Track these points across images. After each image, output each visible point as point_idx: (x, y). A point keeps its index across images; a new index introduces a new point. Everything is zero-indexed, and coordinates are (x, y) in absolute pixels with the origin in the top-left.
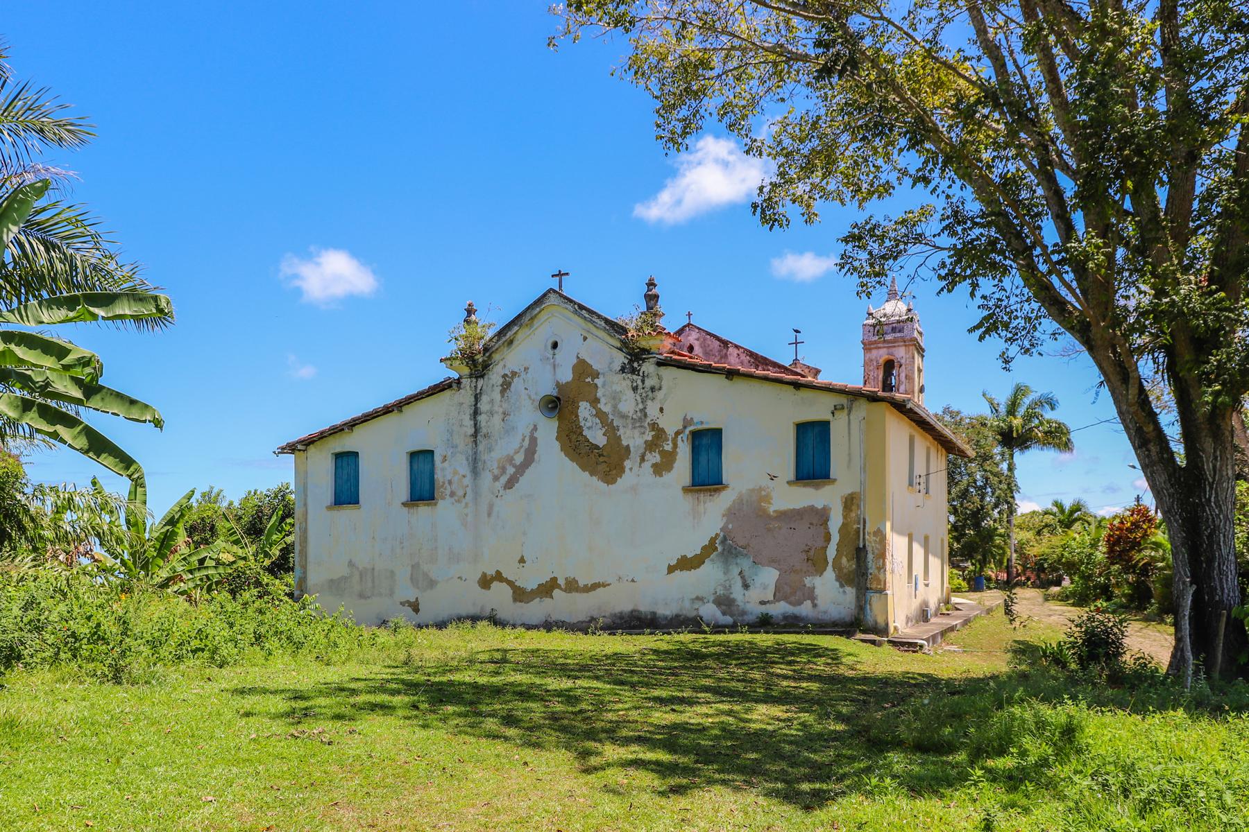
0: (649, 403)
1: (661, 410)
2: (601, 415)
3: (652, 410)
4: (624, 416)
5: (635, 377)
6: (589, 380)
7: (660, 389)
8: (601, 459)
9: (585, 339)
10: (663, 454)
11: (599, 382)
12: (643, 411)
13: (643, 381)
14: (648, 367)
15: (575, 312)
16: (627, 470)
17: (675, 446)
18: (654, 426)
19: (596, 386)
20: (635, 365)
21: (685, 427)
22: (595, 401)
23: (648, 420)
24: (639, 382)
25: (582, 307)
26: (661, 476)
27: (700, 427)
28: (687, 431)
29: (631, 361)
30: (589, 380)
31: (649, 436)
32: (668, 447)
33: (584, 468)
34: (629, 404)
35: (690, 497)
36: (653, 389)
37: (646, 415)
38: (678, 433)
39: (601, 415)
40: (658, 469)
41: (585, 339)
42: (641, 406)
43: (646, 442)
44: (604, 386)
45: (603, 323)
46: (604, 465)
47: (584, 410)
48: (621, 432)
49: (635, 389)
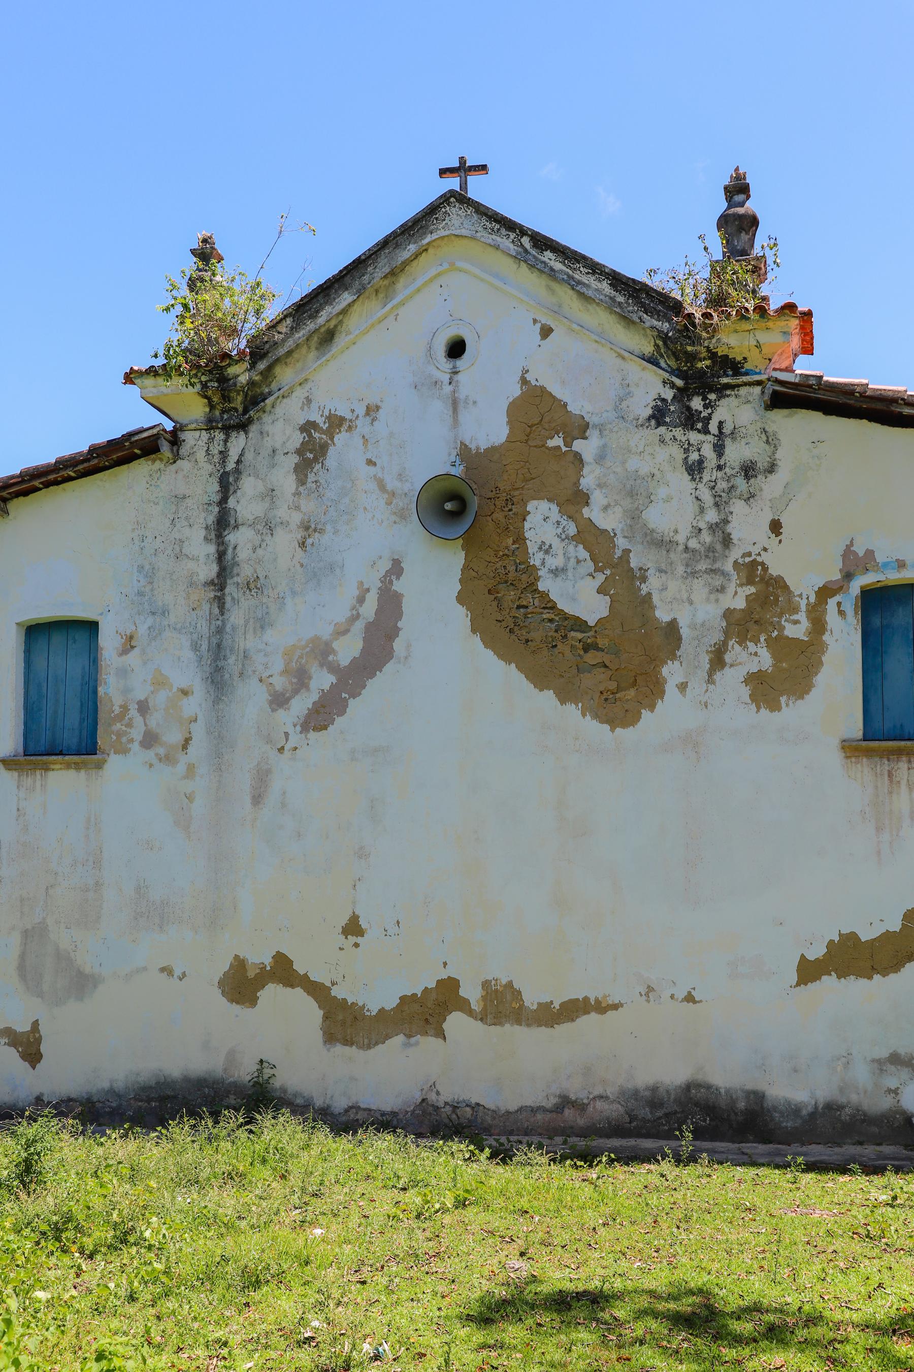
0: (738, 507)
1: (776, 527)
2: (592, 538)
3: (748, 527)
4: (663, 544)
5: (694, 437)
6: (557, 441)
7: (771, 468)
8: (592, 658)
9: (546, 332)
10: (781, 646)
11: (586, 448)
13: (719, 449)
14: (737, 410)
15: (522, 257)
16: (671, 689)
17: (818, 626)
18: (752, 570)
19: (578, 459)
20: (696, 403)
21: (848, 576)
22: (574, 500)
23: (735, 554)
24: (708, 451)
25: (542, 243)
26: (775, 707)
27: (893, 577)
28: (855, 586)
29: (683, 394)
30: (557, 441)
31: (738, 598)
32: (797, 629)
33: (540, 680)
34: (676, 508)
35: (865, 773)
36: (748, 470)
37: (727, 541)
38: (825, 592)
39: (592, 538)
40: (765, 690)
41: (546, 332)
42: (712, 516)
43: (728, 614)
44: (600, 458)
45: (605, 286)
46: (601, 675)
47: (542, 523)
48: (653, 584)
49: (695, 469)
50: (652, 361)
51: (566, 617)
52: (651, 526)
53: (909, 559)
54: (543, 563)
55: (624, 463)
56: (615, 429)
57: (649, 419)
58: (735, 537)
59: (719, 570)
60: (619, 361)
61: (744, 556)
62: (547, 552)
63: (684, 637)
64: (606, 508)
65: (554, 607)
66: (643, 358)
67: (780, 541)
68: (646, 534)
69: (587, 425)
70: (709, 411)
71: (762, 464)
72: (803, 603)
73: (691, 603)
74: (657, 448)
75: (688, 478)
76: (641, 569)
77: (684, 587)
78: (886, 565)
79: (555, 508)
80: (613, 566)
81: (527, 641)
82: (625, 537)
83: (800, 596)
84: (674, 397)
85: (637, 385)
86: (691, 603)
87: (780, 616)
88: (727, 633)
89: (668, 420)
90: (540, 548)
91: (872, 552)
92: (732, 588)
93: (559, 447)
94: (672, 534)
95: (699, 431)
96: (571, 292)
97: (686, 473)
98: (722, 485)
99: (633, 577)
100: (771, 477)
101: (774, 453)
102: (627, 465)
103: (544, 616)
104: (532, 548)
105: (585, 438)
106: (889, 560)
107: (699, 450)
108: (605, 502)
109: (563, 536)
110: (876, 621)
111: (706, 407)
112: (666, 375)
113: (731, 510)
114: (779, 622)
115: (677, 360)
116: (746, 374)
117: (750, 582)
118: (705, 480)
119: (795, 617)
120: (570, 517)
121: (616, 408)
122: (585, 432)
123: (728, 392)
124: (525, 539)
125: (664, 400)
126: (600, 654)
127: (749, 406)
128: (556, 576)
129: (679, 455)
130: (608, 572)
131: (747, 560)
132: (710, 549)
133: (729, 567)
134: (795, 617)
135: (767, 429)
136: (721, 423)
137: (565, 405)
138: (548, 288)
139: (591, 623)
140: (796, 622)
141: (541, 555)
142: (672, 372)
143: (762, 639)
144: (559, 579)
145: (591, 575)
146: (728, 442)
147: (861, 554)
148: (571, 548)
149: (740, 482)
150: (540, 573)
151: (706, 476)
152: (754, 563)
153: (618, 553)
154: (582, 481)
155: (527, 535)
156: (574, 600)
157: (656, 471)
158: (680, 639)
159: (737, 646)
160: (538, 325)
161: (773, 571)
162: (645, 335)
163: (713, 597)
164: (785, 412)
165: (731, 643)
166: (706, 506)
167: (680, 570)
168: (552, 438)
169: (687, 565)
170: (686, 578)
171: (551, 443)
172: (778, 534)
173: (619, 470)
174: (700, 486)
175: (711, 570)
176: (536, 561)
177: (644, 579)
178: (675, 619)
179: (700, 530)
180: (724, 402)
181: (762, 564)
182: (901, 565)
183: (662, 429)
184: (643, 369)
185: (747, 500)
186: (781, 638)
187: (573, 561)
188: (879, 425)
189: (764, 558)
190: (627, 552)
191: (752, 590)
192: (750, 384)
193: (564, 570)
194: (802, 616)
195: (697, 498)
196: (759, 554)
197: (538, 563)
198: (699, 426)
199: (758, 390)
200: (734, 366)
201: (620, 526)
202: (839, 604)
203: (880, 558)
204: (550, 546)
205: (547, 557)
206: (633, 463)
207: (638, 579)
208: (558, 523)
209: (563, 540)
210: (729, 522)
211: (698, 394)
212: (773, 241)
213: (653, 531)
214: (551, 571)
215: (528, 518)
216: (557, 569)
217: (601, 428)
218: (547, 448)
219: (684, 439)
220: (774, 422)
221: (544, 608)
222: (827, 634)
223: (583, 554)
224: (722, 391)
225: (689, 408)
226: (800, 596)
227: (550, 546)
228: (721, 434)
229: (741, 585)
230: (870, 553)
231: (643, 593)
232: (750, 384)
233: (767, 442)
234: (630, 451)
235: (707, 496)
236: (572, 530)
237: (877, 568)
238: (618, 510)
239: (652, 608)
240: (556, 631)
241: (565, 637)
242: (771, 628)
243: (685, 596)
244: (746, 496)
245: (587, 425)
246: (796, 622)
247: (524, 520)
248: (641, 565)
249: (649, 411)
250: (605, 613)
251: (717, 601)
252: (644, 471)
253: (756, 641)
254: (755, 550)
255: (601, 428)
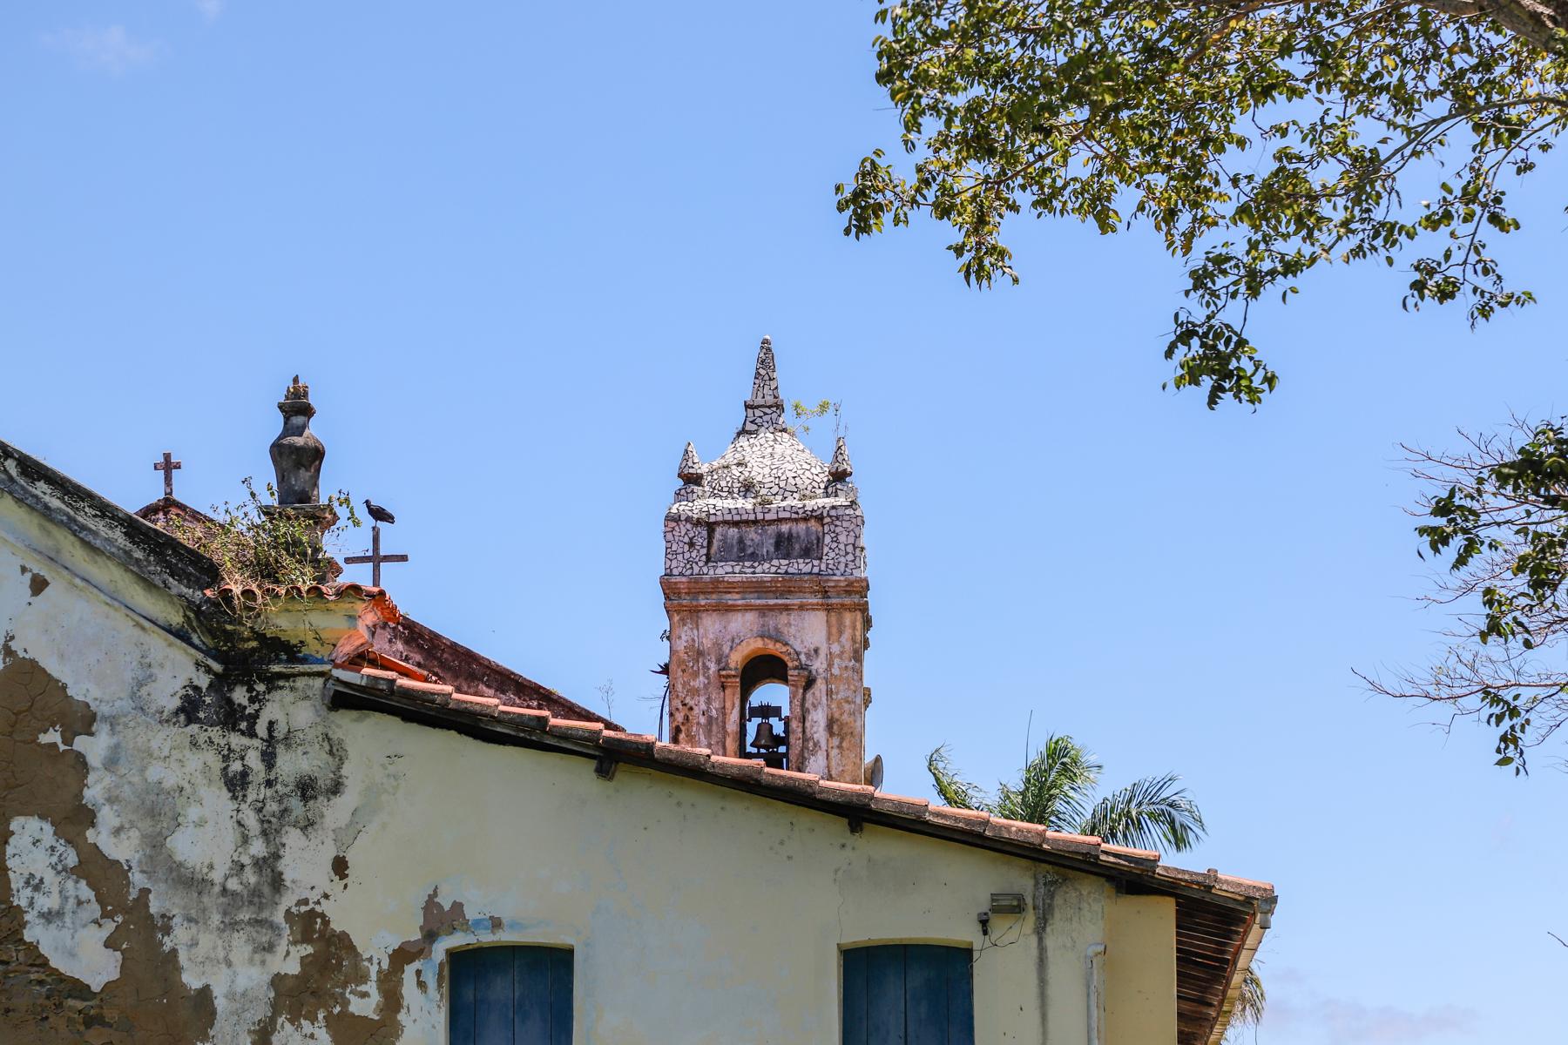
0: (292, 838)
1: (340, 866)
2: (98, 872)
3: (305, 866)
4: (190, 882)
5: (236, 740)
6: (52, 737)
7: (336, 788)
9: (39, 585)
11: (93, 747)
12: (269, 866)
13: (269, 759)
14: (291, 708)
17: (392, 1001)
18: (309, 924)
19: (81, 764)
20: (240, 695)
21: (430, 936)
22: (75, 819)
23: (288, 901)
24: (254, 760)
27: (487, 938)
28: (440, 950)
29: (221, 683)
30: (52, 737)
31: (290, 960)
32: (365, 1004)
34: (210, 836)
36: (306, 788)
37: (277, 883)
38: (402, 956)
39: (98, 872)
41: (39, 585)
42: (258, 848)
43: (277, 981)
44: (111, 763)
48: (180, 936)
49: (236, 784)
50: (181, 635)
51: (61, 978)
52: (178, 858)
53: (505, 915)
54: (31, 904)
55: (143, 770)
56: (132, 724)
57: (177, 713)
58: (288, 877)
59: (266, 921)
60: (137, 631)
61: (299, 903)
62: (37, 888)
63: (219, 1010)
64: (117, 831)
65: (44, 963)
66: (168, 630)
67: (346, 886)
68: (171, 870)
69: (92, 718)
70: (256, 706)
71: (324, 781)
72: (374, 970)
73: (229, 964)
74: (187, 752)
75: (226, 794)
76: (163, 916)
77: (220, 942)
78: (478, 923)
79: (48, 828)
80: (126, 911)
81: (7, 1011)
82: (142, 872)
83: (370, 960)
84: (211, 685)
85: (162, 666)
86: (229, 964)
87: (344, 987)
88: (276, 1008)
89: (202, 715)
90: (27, 883)
91: (461, 905)
92: (282, 948)
93: (54, 745)
94: (205, 870)
95: (243, 733)
96: (72, 538)
97: (225, 790)
98: (272, 807)
99: (154, 927)
100: (336, 800)
101: (339, 768)
102: (148, 773)
103: (32, 977)
104: (16, 882)
105: (92, 734)
106: (481, 916)
107: (242, 758)
108: (116, 822)
109: (60, 868)
110: (469, 994)
111: (252, 700)
112: (200, 656)
113: (284, 840)
114: (343, 994)
115: (214, 638)
116: (304, 661)
117: (306, 939)
118: (249, 800)
119: (363, 988)
120: (68, 842)
121: (133, 696)
122: (91, 725)
123: (281, 683)
124: (7, 869)
125: (196, 689)
126: (107, 1030)
127: (307, 703)
128: (49, 922)
129: (216, 764)
130: (120, 919)
131: (303, 909)
132: (255, 893)
133: (279, 918)
134: (363, 988)
135: (330, 735)
136: (271, 723)
137: (64, 687)
138: (42, 528)
139: (96, 988)
140: (365, 995)
141: (28, 892)
142: (207, 653)
143: (320, 1016)
144: (53, 926)
145: (96, 922)
146: (280, 749)
147: (447, 908)
148: (70, 884)
149: (295, 803)
150: (27, 917)
151: (251, 796)
152: (312, 914)
153: (134, 894)
154: (87, 793)
155: (9, 864)
156: (72, 955)
157: (186, 785)
158: (213, 1013)
159: (287, 1025)
160: (28, 576)
161: (336, 926)
162: (172, 603)
163: (257, 957)
164: (354, 714)
165: (280, 1021)
166: (251, 834)
167: (216, 919)
168: (45, 731)
169: (225, 914)
170: (223, 931)
171: (44, 739)
172: (343, 876)
173: (136, 779)
174: (243, 806)
175: (257, 921)
176: (21, 900)
177: (167, 930)
178: (208, 986)
179: (243, 866)
180: (276, 695)
181: (323, 916)
182: (496, 924)
183: (194, 728)
184: (170, 645)
185: (304, 829)
186: (346, 1015)
187: (72, 902)
188: (470, 740)
189: (325, 907)
190: (145, 892)
191: (309, 949)
192: (309, 675)
193: (60, 914)
194: (371, 987)
195: (239, 823)
196: (318, 903)
197: (23, 903)
198: (243, 725)
199: (319, 682)
200: (290, 651)
201: (137, 856)
202: (419, 973)
203: (471, 914)
204: (41, 880)
205: (36, 895)
206: (155, 772)
207: (161, 929)
208: (53, 848)
209: (59, 873)
210: (279, 857)
211: (243, 683)
212: (343, 497)
213: (180, 865)
214: (42, 915)
215: (12, 840)
216: (50, 912)
217: (113, 721)
218: (39, 745)
219: (223, 742)
220: (339, 726)
221: (32, 965)
222: (403, 1011)
223: (86, 892)
224: (272, 681)
225: (230, 702)
226: (370, 960)
227: (41, 880)
228: (271, 740)
229: (295, 943)
230: (458, 907)
231: (166, 949)
232: (309, 675)
233: (331, 753)
234: (151, 755)
235: (251, 820)
236: (72, 859)
237: (466, 926)
238: (134, 833)
239: (178, 969)
240: (48, 998)
241: (59, 1006)
242: (332, 1003)
243: (221, 954)
244: (302, 824)
245: (92, 718)
246: (365, 995)
247: (6, 842)
248: (163, 911)
249: (176, 703)
250: (115, 975)
251: (263, 962)
252: (170, 782)
253: (313, 1019)
254: (314, 896)
255: (113, 721)
